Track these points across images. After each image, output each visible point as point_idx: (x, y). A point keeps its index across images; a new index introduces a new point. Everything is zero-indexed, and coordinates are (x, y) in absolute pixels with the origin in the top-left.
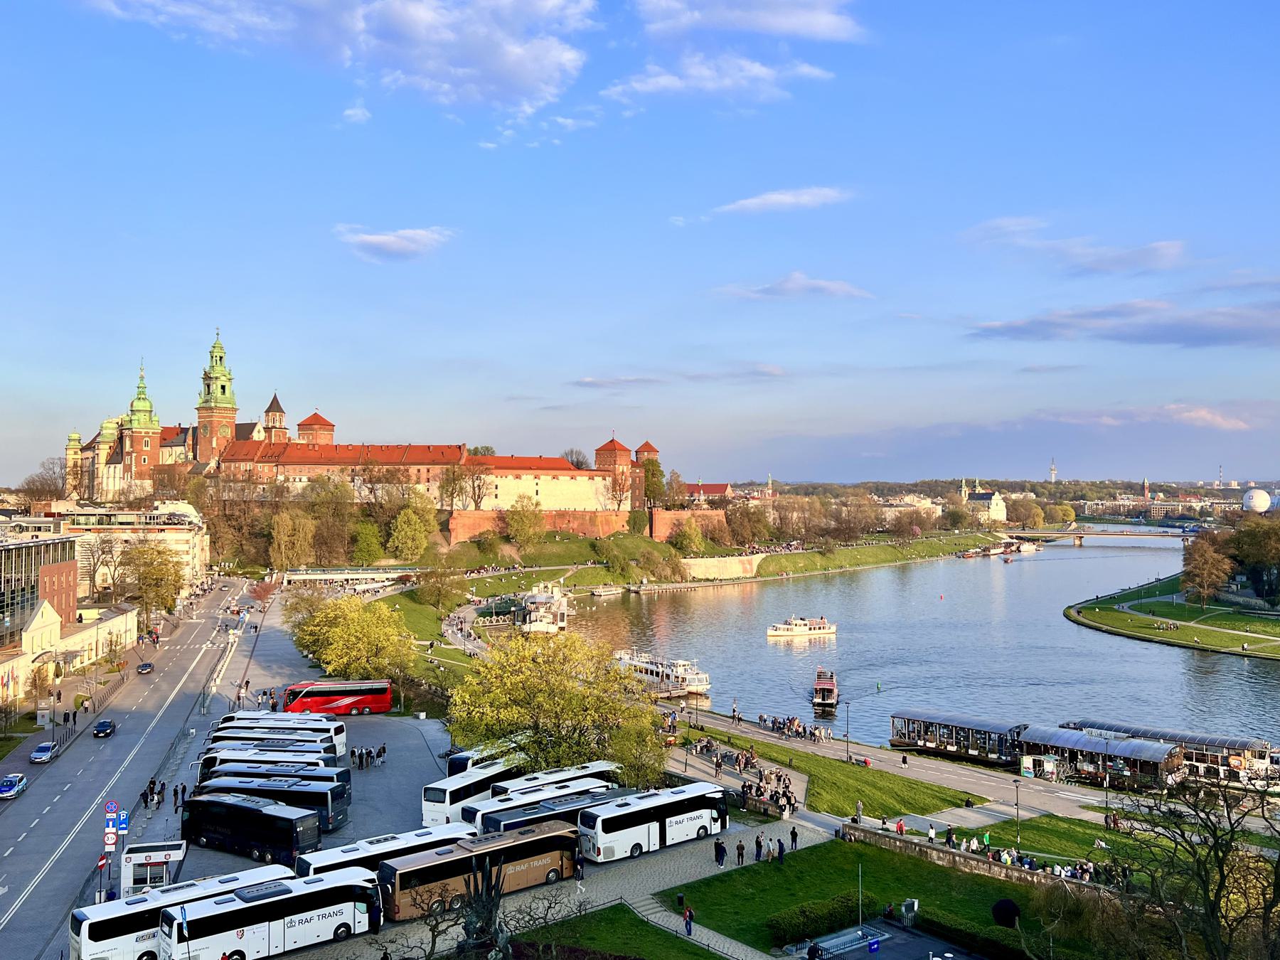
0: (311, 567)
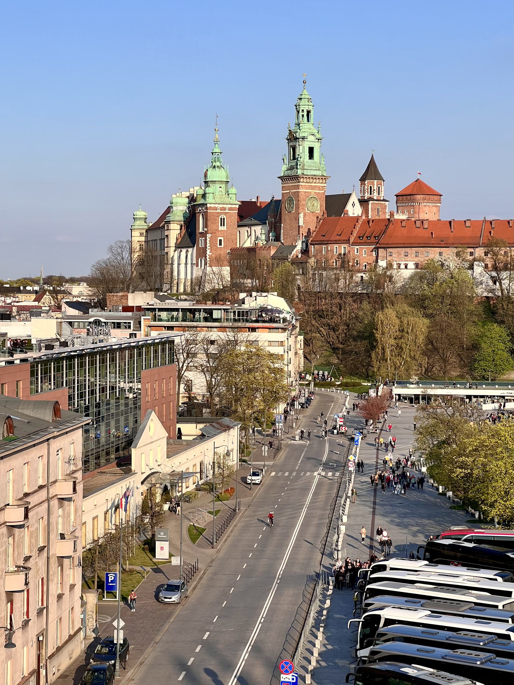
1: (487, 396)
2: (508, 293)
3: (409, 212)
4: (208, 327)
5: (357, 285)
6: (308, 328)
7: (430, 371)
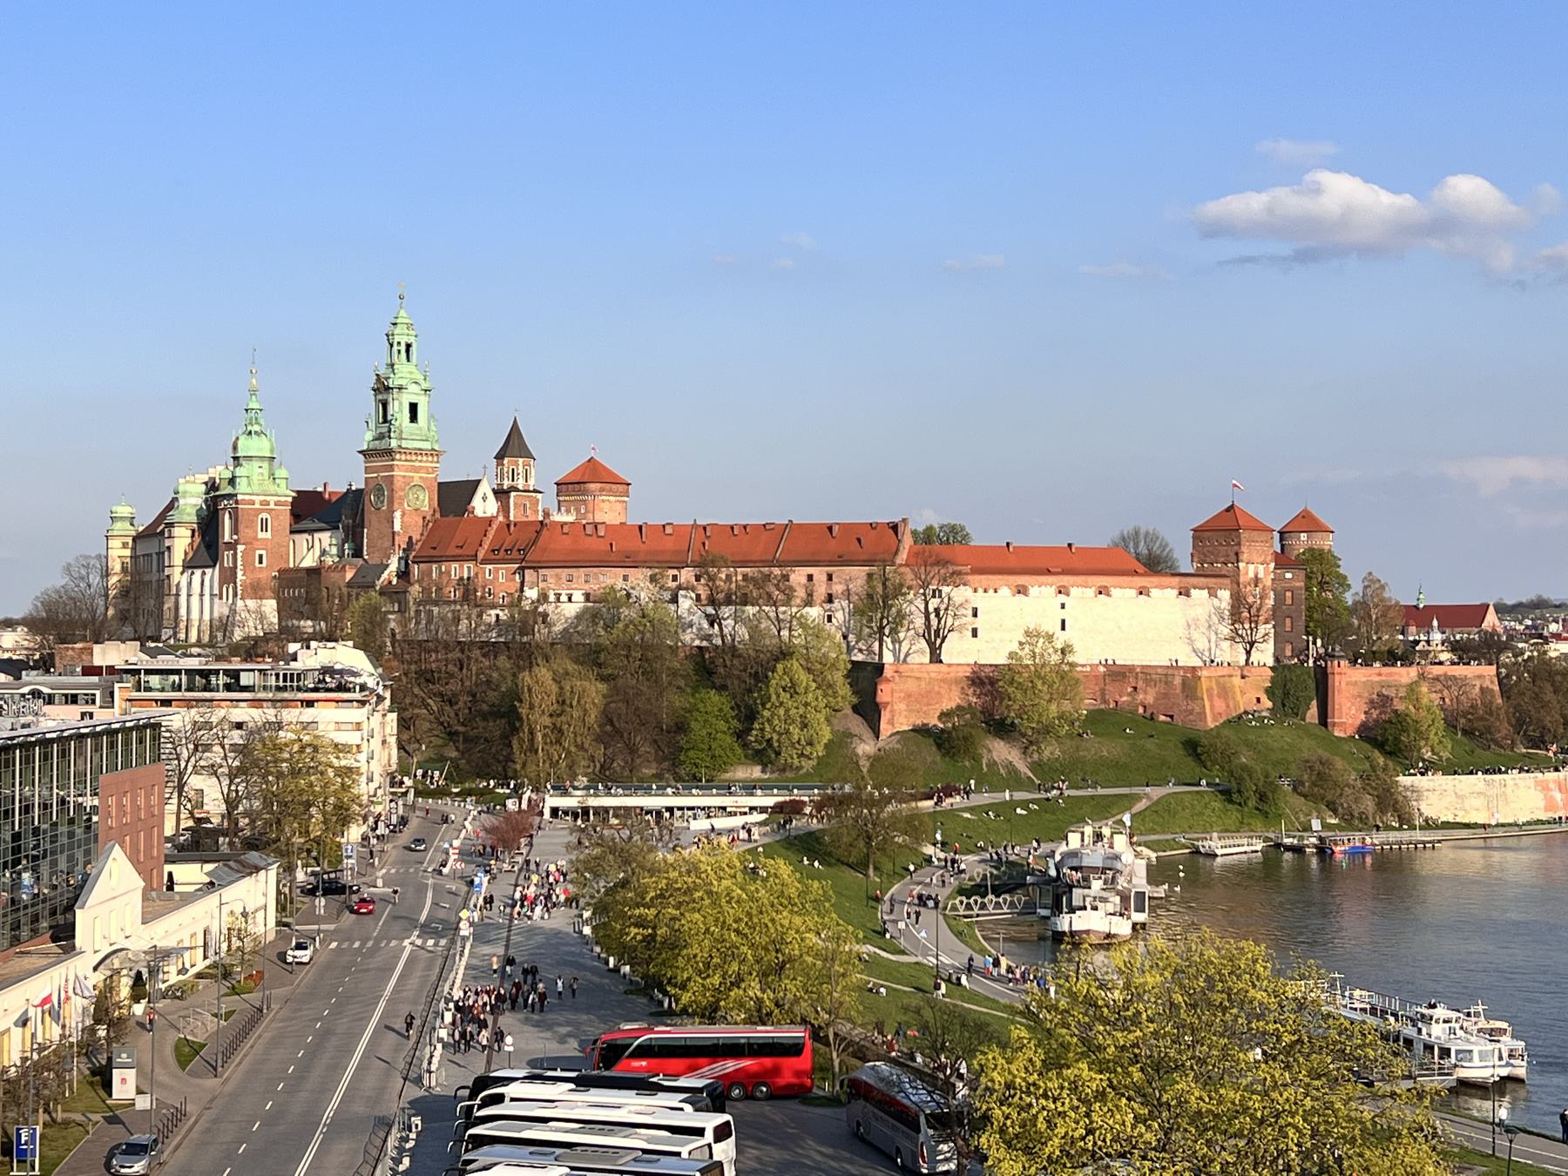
0: (591, 787)
1: (699, 808)
2: (733, 640)
3: (578, 510)
4: (232, 701)
5: (490, 628)
6: (408, 701)
7: (609, 769)
